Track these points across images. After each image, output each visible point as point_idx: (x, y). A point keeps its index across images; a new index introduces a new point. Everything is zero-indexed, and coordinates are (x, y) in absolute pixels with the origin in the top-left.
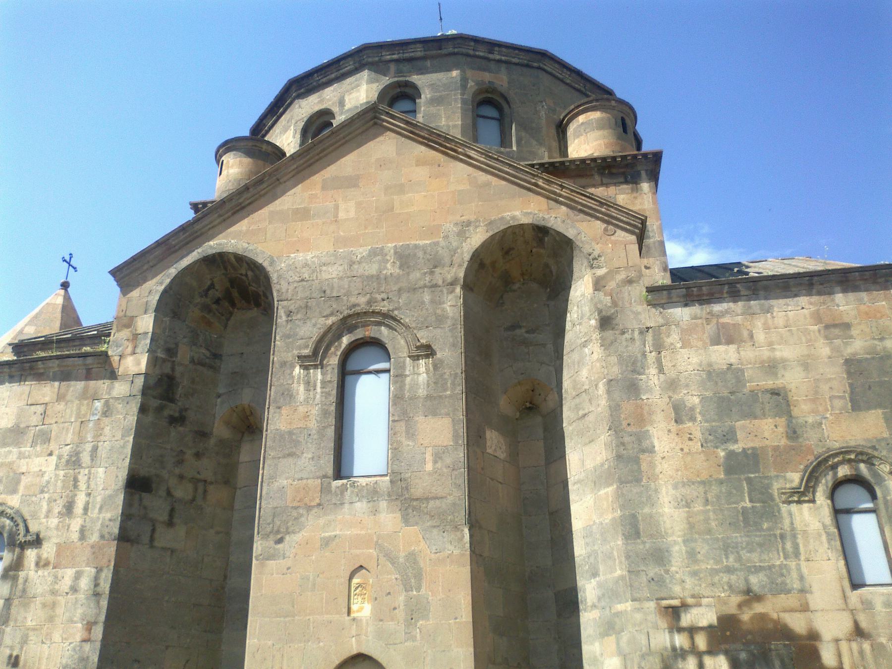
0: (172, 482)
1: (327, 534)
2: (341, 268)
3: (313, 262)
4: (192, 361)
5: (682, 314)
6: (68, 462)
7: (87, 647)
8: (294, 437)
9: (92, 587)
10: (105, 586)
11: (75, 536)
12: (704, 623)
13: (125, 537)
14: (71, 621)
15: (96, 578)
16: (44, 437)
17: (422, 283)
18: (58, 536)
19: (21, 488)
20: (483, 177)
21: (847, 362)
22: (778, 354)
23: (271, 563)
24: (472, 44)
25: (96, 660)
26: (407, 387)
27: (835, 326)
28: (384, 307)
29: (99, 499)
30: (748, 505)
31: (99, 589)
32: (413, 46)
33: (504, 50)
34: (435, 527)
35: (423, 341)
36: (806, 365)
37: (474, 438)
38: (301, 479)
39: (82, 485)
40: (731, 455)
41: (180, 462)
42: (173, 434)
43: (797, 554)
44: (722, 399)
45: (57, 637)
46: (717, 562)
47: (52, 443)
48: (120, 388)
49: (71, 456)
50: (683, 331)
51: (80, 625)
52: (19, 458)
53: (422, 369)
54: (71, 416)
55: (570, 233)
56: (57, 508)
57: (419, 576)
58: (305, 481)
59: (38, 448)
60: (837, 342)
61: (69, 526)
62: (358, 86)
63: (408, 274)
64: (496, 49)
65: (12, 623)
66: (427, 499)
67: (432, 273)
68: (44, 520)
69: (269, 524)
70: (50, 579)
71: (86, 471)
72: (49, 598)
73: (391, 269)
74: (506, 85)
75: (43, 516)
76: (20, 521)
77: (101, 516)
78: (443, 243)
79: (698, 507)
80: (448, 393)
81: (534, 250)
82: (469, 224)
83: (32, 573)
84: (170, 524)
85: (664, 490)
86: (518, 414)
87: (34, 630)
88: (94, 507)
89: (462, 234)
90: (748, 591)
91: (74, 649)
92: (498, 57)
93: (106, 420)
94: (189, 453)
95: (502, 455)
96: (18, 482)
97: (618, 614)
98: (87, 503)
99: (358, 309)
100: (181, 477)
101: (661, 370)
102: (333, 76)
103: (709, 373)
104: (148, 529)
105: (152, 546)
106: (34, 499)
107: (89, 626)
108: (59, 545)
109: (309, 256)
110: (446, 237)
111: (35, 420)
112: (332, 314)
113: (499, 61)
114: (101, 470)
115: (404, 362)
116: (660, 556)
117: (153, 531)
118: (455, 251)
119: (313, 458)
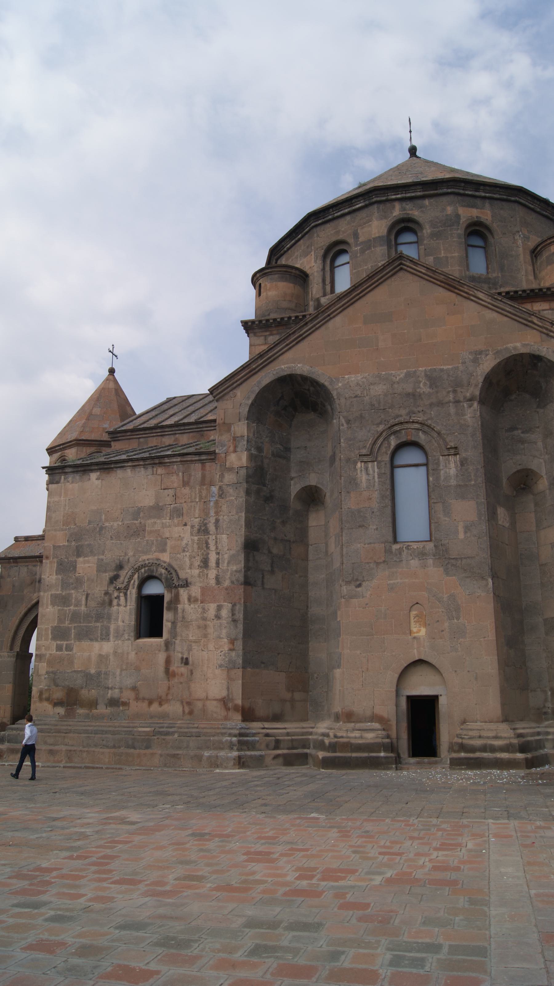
1: (392, 582)
2: (384, 387)
3: (363, 382)
4: (273, 454)
6: (199, 530)
7: (233, 654)
8: (362, 514)
9: (231, 615)
10: (240, 616)
11: (213, 582)
13: (247, 583)
14: (219, 637)
16: (178, 513)
20: (490, 315)
23: (354, 601)
24: (463, 184)
25: (241, 662)
26: (442, 478)
28: (420, 418)
29: (226, 556)
31: (236, 617)
32: (413, 188)
33: (488, 188)
34: (467, 577)
35: (452, 444)
37: (492, 515)
38: (370, 543)
39: (212, 547)
42: (267, 509)
45: (211, 646)
48: (229, 478)
49: (200, 526)
51: (226, 640)
52: (163, 527)
53: (452, 465)
54: (195, 498)
56: (197, 562)
58: (373, 545)
59: (176, 521)
61: (207, 575)
62: (370, 221)
63: (437, 392)
64: (482, 187)
65: (179, 638)
67: (455, 391)
68: (189, 571)
69: (350, 574)
70: (200, 610)
72: (201, 622)
73: (424, 388)
74: (489, 218)
75: (187, 568)
76: (172, 571)
78: (461, 367)
80: (473, 482)
81: (529, 371)
82: (481, 353)
83: (187, 606)
84: (272, 572)
86: (515, 492)
87: (195, 642)
89: (475, 361)
91: (225, 655)
92: (483, 194)
95: (507, 525)
96: (166, 544)
99: (402, 419)
100: (275, 539)
102: (346, 211)
104: (261, 576)
105: (263, 588)
106: (178, 556)
107: (232, 642)
108: (202, 588)
109: (359, 377)
110: (464, 363)
111: (169, 500)
113: (484, 198)
114: (224, 536)
115: (439, 459)
117: (263, 577)
118: (472, 375)
119: (377, 529)
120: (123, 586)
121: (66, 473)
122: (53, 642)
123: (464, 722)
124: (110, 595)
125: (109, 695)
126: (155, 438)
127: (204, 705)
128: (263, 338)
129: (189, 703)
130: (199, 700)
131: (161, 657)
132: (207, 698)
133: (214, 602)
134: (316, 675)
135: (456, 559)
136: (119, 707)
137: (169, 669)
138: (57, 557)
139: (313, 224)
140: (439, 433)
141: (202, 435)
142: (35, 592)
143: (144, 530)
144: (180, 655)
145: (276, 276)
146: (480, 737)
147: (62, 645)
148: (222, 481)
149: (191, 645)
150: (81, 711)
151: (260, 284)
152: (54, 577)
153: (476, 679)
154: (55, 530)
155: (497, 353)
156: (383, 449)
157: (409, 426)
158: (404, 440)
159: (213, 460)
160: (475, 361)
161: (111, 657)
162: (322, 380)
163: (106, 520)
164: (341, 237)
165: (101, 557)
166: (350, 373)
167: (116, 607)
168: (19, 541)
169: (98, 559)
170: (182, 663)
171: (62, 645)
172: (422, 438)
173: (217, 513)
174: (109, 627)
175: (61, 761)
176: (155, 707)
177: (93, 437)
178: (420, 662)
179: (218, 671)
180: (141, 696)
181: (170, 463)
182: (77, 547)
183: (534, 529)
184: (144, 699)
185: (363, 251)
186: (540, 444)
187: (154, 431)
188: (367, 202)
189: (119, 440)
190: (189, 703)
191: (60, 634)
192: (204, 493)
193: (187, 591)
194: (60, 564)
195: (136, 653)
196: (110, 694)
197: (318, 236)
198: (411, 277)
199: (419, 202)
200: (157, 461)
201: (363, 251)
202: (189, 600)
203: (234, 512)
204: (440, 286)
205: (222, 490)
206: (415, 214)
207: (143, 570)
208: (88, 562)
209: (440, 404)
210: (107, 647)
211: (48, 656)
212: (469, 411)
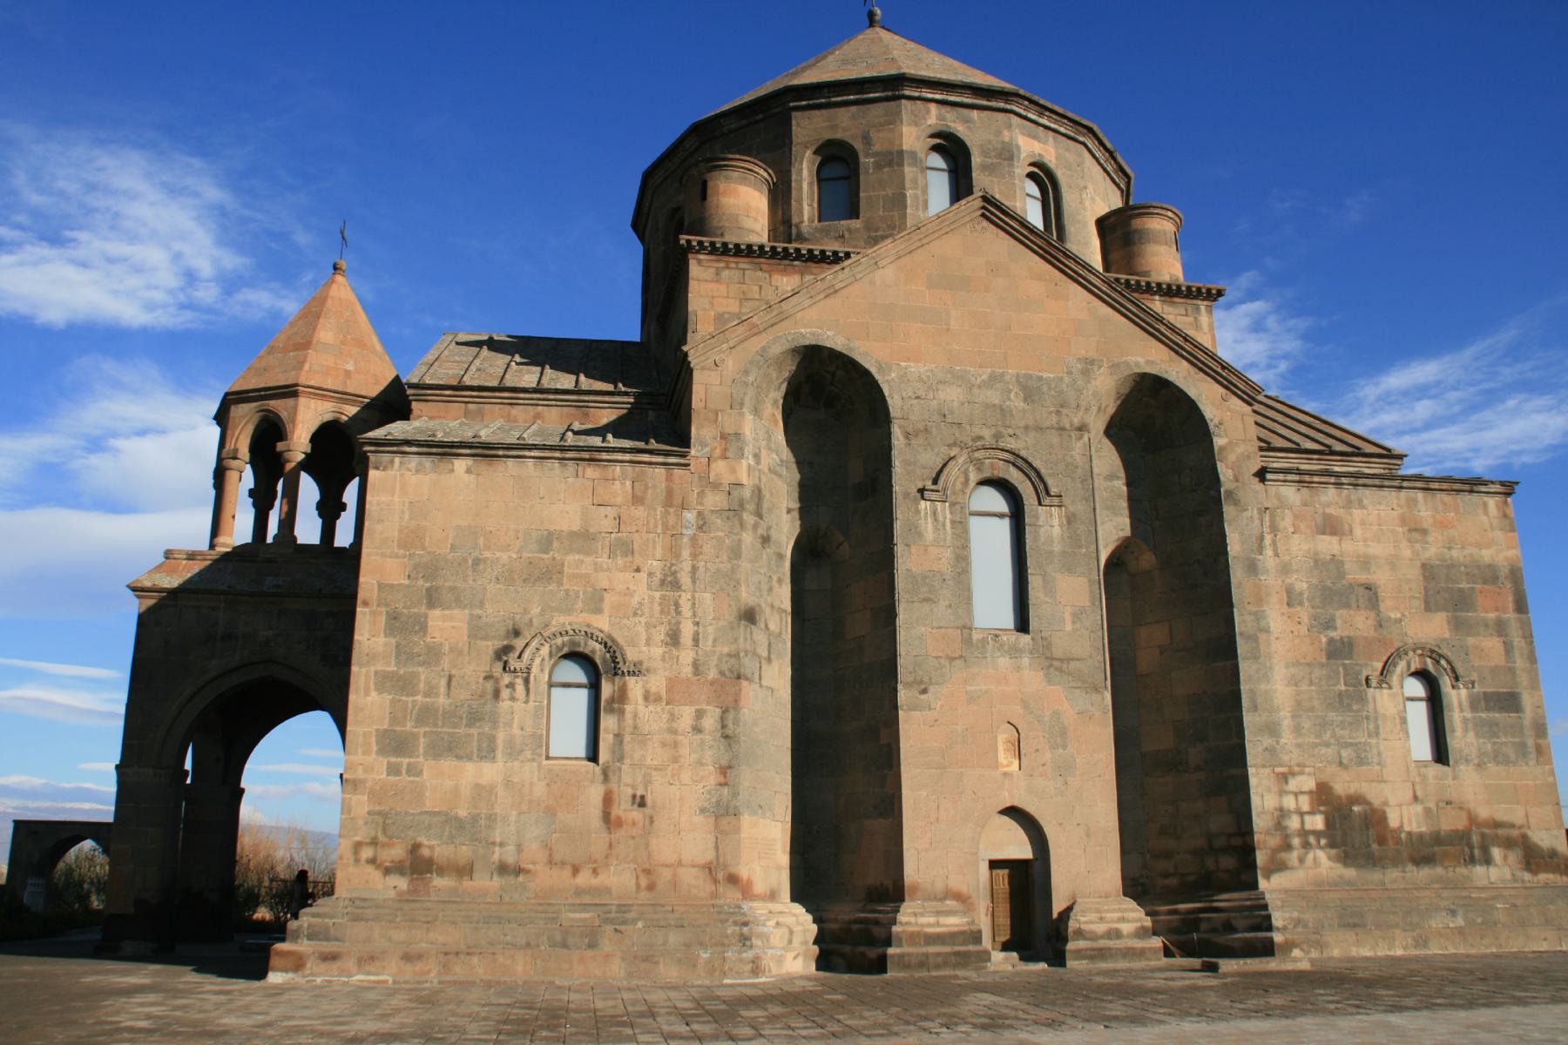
0: (768, 611)
6: (663, 582)
7: (725, 790)
11: (687, 671)
12: (1306, 788)
14: (702, 764)
15: (722, 719)
16: (627, 549)
17: (1047, 424)
19: (606, 606)
21: (1423, 565)
22: (1371, 551)
27: (1416, 530)
28: (1011, 444)
29: (710, 629)
30: (1343, 688)
31: (729, 732)
36: (1393, 562)
39: (686, 611)
40: (1331, 641)
41: (770, 589)
43: (1377, 734)
44: (1325, 588)
45: (686, 777)
47: (637, 556)
48: (714, 500)
50: (1296, 517)
53: (1056, 522)
55: (1192, 393)
56: (660, 634)
57: (1063, 733)
60: (1418, 546)
65: (627, 761)
66: (1069, 660)
67: (1058, 412)
70: (665, 716)
73: (1017, 403)
78: (1067, 379)
79: (1304, 687)
82: (1092, 362)
83: (641, 708)
88: (706, 639)
89: (1085, 373)
90: (1341, 763)
94: (775, 578)
96: (601, 600)
98: (697, 634)
100: (772, 607)
103: (1316, 561)
112: (955, 444)
114: (707, 595)
116: (1272, 729)
118: (1080, 391)
124: (497, 681)
125: (496, 857)
127: (675, 875)
128: (712, 270)
129: (647, 872)
131: (596, 793)
132: (680, 864)
133: (691, 703)
138: (387, 605)
141: (587, 414)
144: (630, 791)
147: (400, 764)
148: (701, 504)
152: (382, 640)
153: (1088, 835)
154: (383, 555)
160: (1085, 373)
161: (501, 792)
163: (487, 548)
165: (479, 612)
166: (909, 360)
169: (471, 615)
171: (400, 764)
172: (1014, 476)
173: (694, 556)
174: (494, 737)
175: (429, 972)
176: (584, 879)
177: (329, 383)
179: (699, 819)
180: (557, 857)
184: (563, 863)
185: (878, 167)
190: (647, 872)
191: (394, 744)
192: (672, 520)
194: (394, 617)
196: (497, 855)
199: (965, 111)
200: (586, 455)
201: (878, 167)
202: (646, 698)
206: (960, 129)
209: (1039, 429)
210: (490, 772)
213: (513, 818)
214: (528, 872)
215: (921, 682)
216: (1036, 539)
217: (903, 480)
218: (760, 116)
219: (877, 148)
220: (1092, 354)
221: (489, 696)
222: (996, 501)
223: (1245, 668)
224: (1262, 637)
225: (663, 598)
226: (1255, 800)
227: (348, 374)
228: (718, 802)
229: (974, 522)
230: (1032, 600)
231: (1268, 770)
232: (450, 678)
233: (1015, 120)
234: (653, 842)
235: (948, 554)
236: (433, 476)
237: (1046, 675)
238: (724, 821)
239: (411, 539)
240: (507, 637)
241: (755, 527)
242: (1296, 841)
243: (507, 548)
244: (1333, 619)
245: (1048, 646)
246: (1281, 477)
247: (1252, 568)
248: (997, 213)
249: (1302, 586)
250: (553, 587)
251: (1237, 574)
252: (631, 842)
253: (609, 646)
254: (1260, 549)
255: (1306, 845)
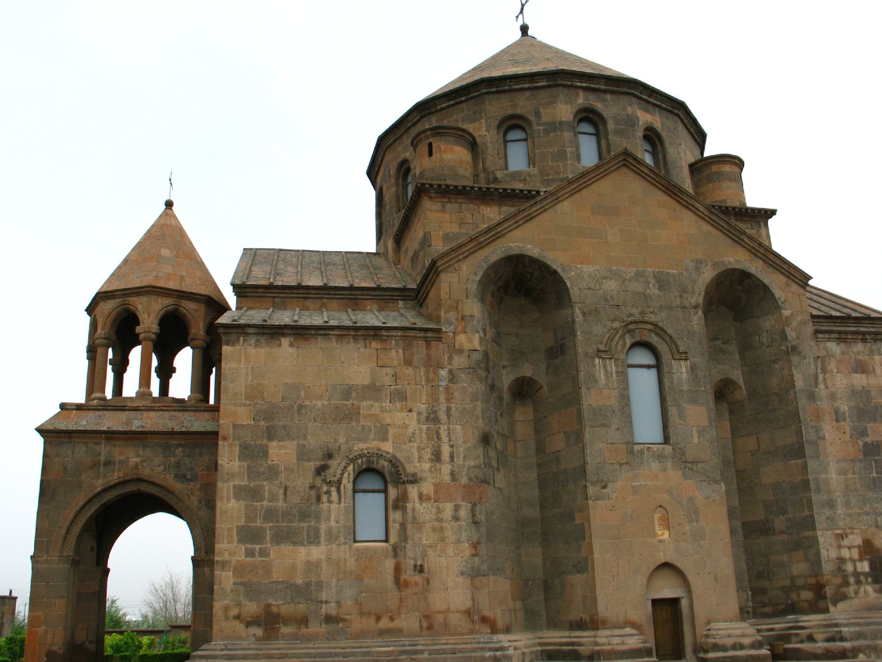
0: (496, 436)
3: (596, 275)
5: (834, 347)
6: (427, 418)
7: (477, 559)
11: (447, 478)
14: (460, 542)
16: (401, 396)
17: (674, 304)
18: (433, 478)
20: (707, 227)
26: (675, 382)
28: (653, 318)
29: (461, 450)
30: (875, 475)
31: (477, 519)
38: (613, 443)
39: (445, 439)
40: (865, 444)
41: (496, 421)
45: (450, 551)
46: (861, 508)
47: (408, 399)
48: (459, 361)
49: (429, 414)
50: (838, 362)
53: (684, 370)
54: (421, 380)
55: (766, 281)
56: (427, 455)
57: (696, 512)
65: (410, 542)
66: (697, 462)
67: (681, 296)
68: (418, 464)
70: (434, 510)
71: (446, 427)
73: (653, 290)
77: (467, 463)
78: (685, 274)
79: (850, 476)
83: (417, 505)
85: (831, 464)
88: (459, 457)
89: (697, 269)
90: (877, 526)
91: (466, 561)
93: (454, 386)
96: (387, 432)
97: (806, 538)
100: (498, 433)
101: (827, 387)
102: (527, 85)
106: (404, 446)
107: (475, 546)
110: (687, 270)
111: (387, 380)
113: (655, 105)
116: (831, 504)
119: (618, 429)
120: (336, 479)
121: (247, 334)
122: (240, 545)
123: (709, 623)
124: (318, 489)
125: (323, 610)
126: (295, 300)
127: (445, 619)
129: (427, 617)
130: (440, 612)
131: (389, 564)
132: (448, 610)
133: (451, 501)
134: (530, 582)
135: (692, 463)
136: (338, 623)
137: (399, 578)
138: (239, 439)
139: (485, 91)
140: (671, 337)
142: (98, 478)
143: (358, 413)
144: (412, 562)
145: (452, 139)
146: (729, 636)
148: (450, 364)
149: (426, 550)
150: (285, 630)
151: (430, 145)
152: (237, 463)
153: (716, 581)
154: (235, 405)
155: (715, 265)
156: (620, 347)
157: (640, 326)
158: (638, 339)
159: (439, 339)
160: (697, 269)
161: (324, 565)
162: (554, 266)
164: (519, 111)
165: (303, 442)
167: (326, 504)
168: (67, 409)
169: (298, 445)
170: (415, 571)
172: (655, 340)
173: (448, 400)
177: (172, 285)
178: (666, 565)
179: (460, 580)
181: (387, 336)
182: (267, 428)
183: (729, 436)
184: (370, 614)
186: (737, 356)
187: (295, 291)
188: (552, 83)
189: (247, 297)
190: (427, 617)
191: (249, 535)
192: (431, 375)
193: (416, 488)
194: (244, 447)
195: (357, 560)
196: (324, 609)
197: (490, 104)
198: (632, 174)
199: (602, 95)
203: (468, 400)
204: (660, 189)
205: (452, 374)
206: (599, 106)
207: (360, 461)
208: (285, 447)
209: (670, 308)
210: (317, 553)
211: (233, 563)
212: (695, 318)
213: (333, 584)
214: (345, 620)
215: (602, 481)
216: (672, 382)
217: (582, 344)
218: (463, 98)
219: (544, 119)
220: (700, 256)
221: (314, 500)
222: (643, 357)
223: (812, 464)
224: (821, 442)
225: (428, 429)
226: (823, 552)
227: (182, 278)
228: (473, 568)
229: (632, 372)
230: (671, 423)
231: (830, 532)
232: (286, 488)
233: (634, 100)
234: (430, 596)
235: (615, 393)
236: (267, 349)
237: (684, 474)
238: (477, 580)
239: (254, 393)
240: (323, 459)
241: (486, 378)
242: (852, 580)
243: (320, 397)
244: (866, 430)
245: (684, 454)
246: (827, 336)
247: (812, 397)
248: (628, 160)
249: (844, 408)
250: (354, 424)
251: (803, 401)
252: (415, 597)
253: (394, 463)
254: (816, 384)
255: (858, 582)
